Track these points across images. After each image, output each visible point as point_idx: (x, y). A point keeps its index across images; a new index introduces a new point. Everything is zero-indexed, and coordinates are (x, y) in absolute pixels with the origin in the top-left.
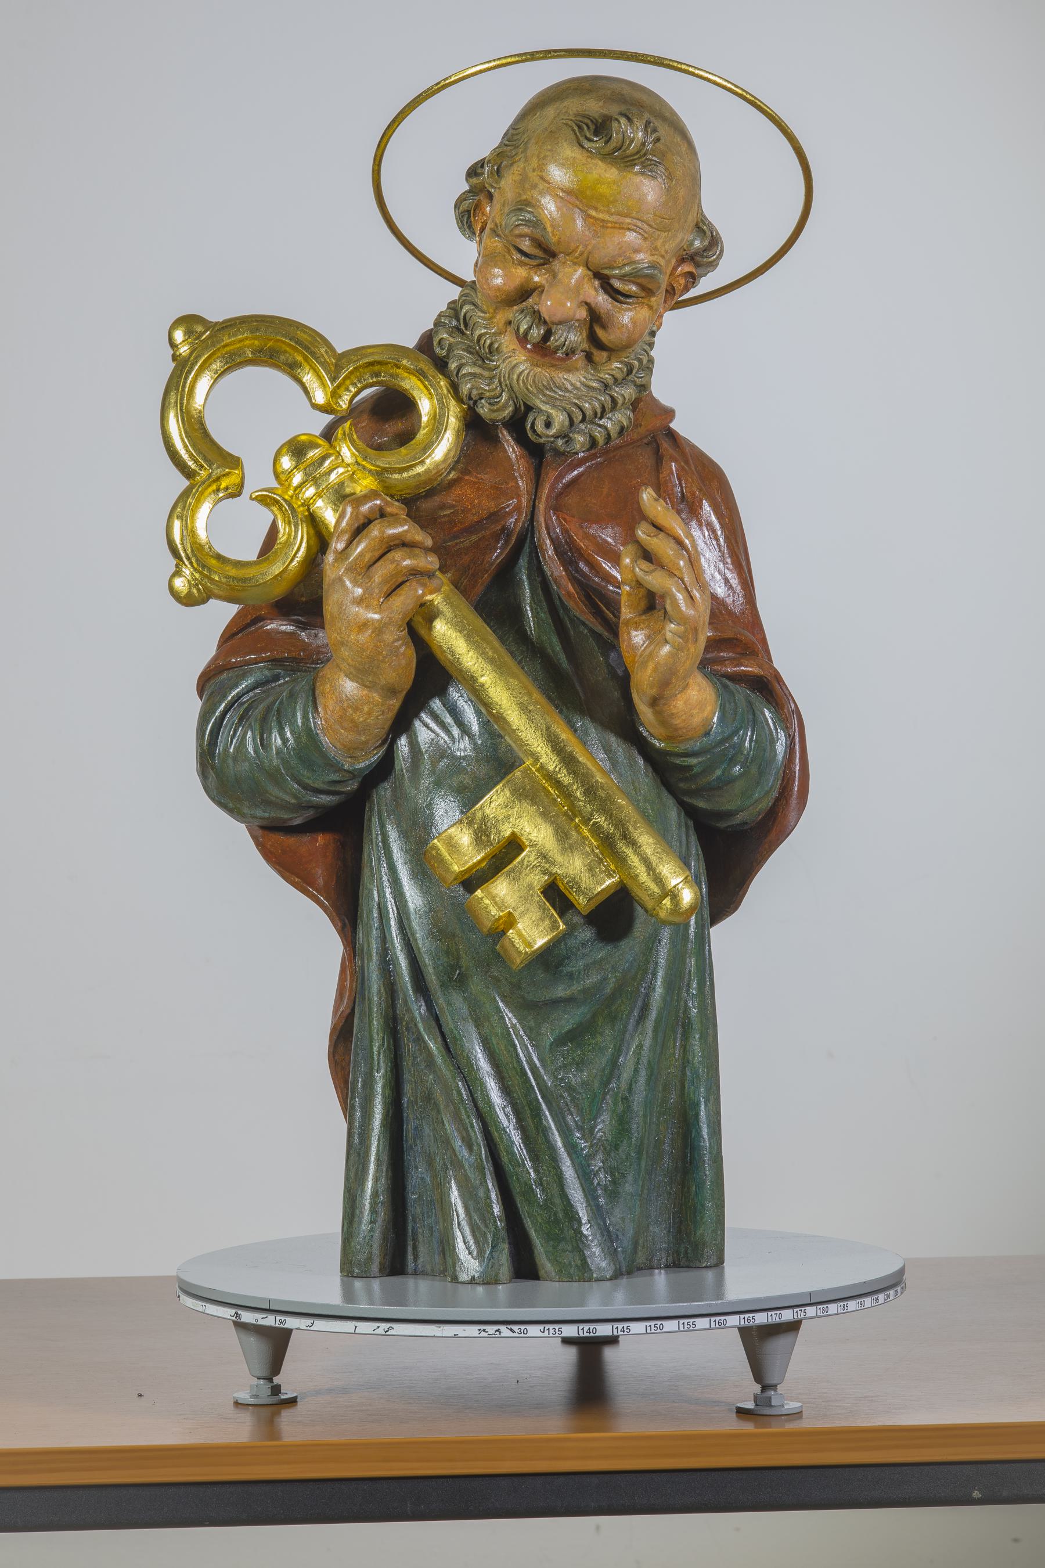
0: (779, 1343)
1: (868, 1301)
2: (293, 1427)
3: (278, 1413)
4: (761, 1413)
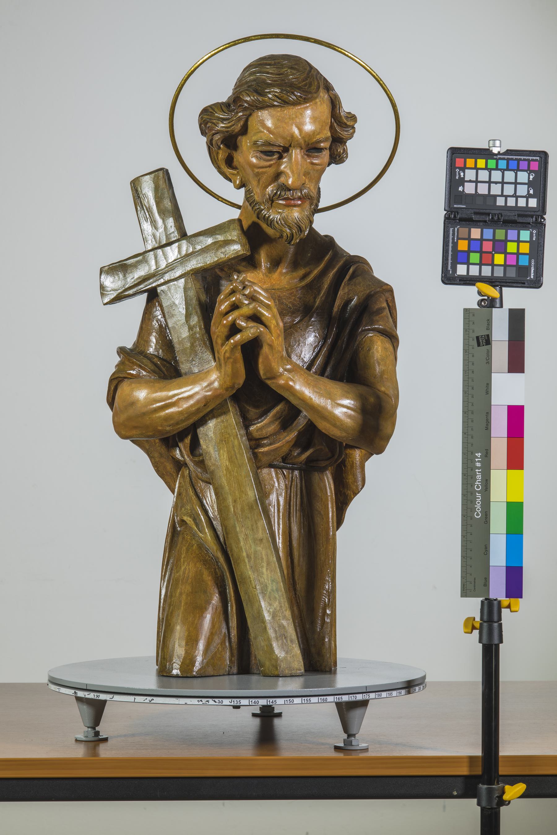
0: (357, 713)
4: (347, 748)
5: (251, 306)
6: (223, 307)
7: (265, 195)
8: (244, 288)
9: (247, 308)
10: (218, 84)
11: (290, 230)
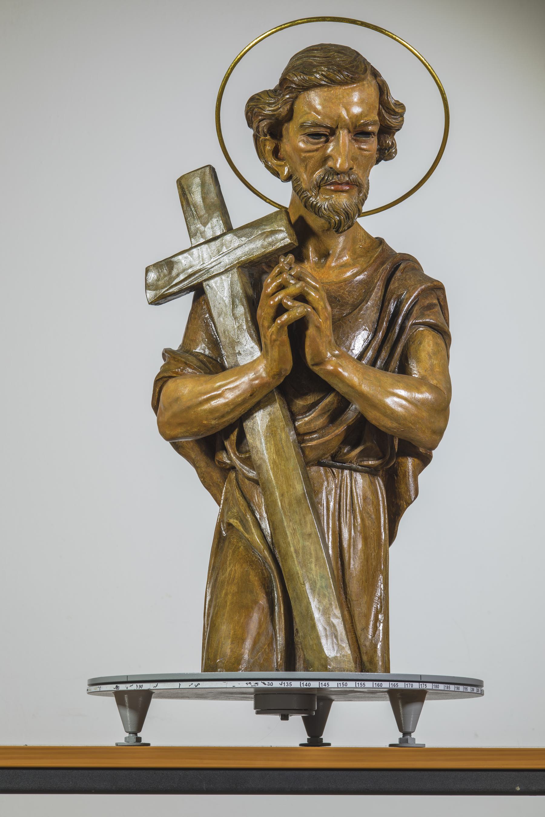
5: (298, 286)
6: (269, 290)
7: (312, 181)
8: (290, 268)
9: (294, 288)
10: (264, 73)
11: (338, 216)
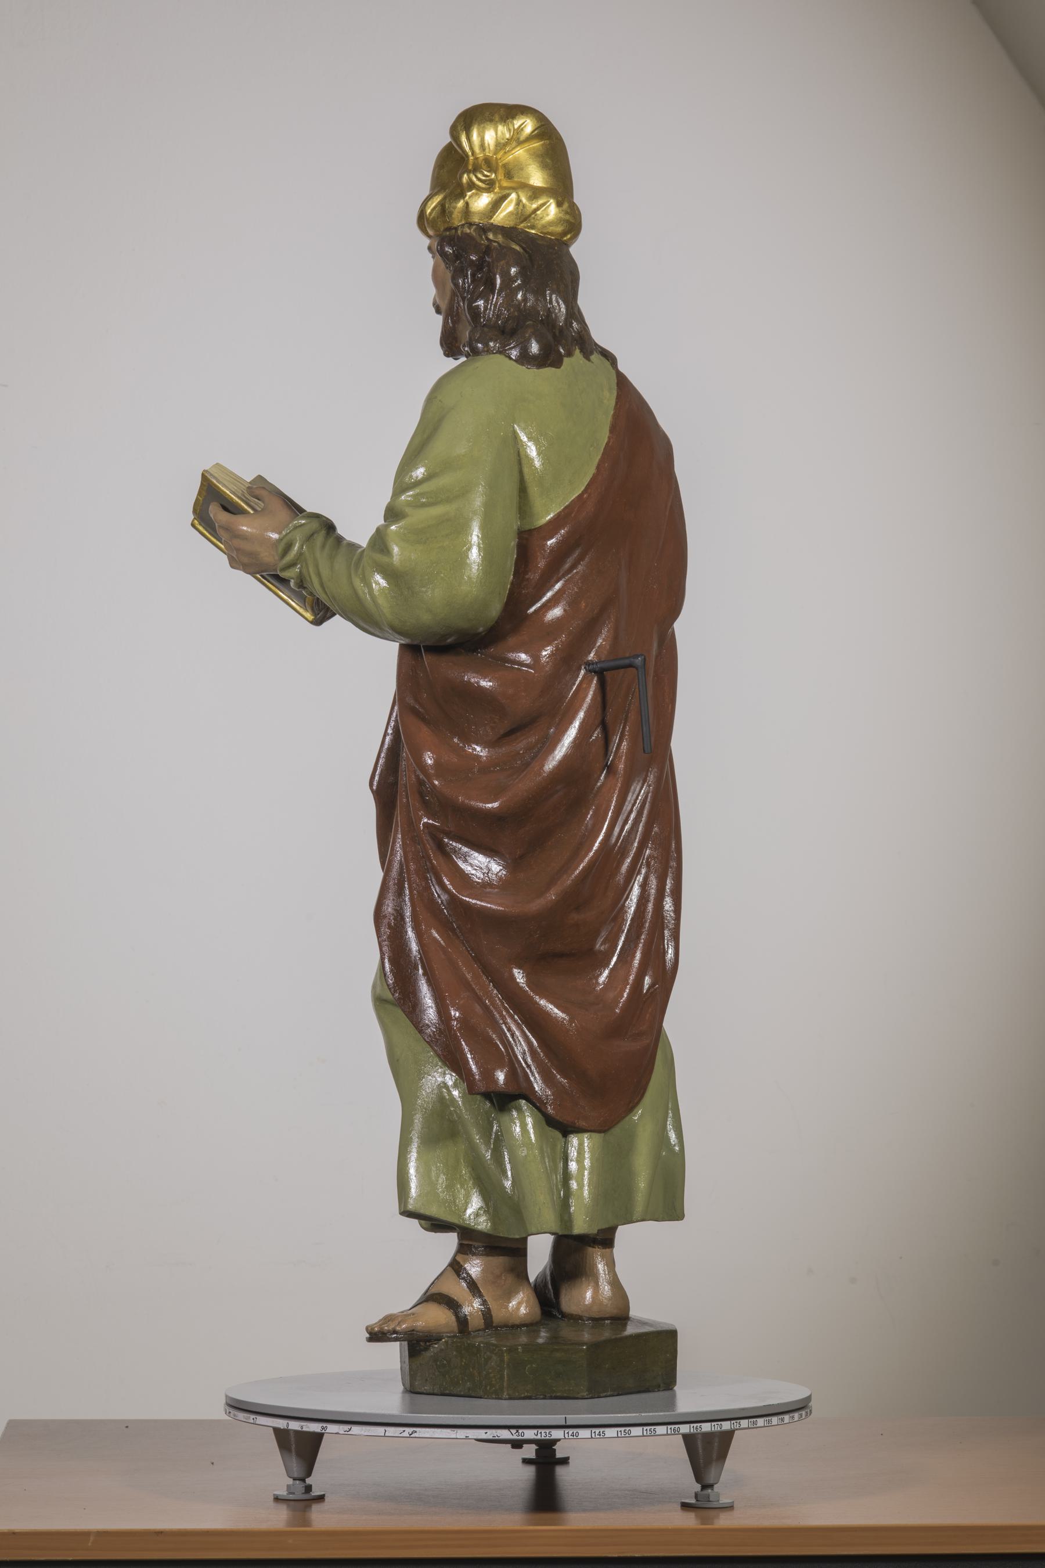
1: (787, 1418)
2: (321, 1518)
3: (310, 1506)
